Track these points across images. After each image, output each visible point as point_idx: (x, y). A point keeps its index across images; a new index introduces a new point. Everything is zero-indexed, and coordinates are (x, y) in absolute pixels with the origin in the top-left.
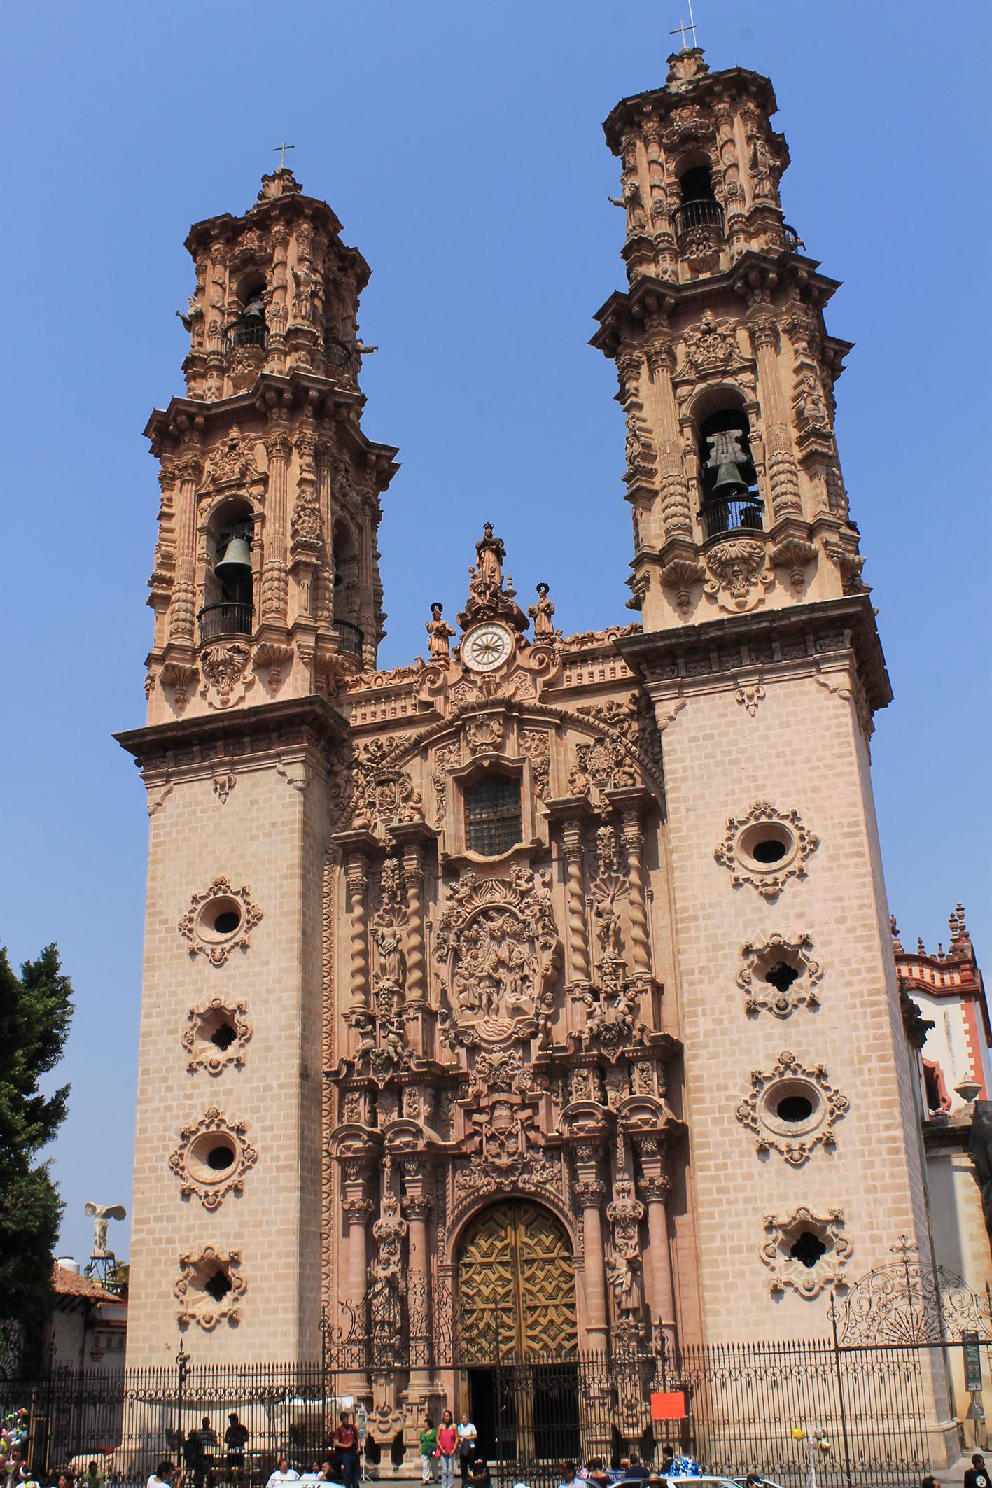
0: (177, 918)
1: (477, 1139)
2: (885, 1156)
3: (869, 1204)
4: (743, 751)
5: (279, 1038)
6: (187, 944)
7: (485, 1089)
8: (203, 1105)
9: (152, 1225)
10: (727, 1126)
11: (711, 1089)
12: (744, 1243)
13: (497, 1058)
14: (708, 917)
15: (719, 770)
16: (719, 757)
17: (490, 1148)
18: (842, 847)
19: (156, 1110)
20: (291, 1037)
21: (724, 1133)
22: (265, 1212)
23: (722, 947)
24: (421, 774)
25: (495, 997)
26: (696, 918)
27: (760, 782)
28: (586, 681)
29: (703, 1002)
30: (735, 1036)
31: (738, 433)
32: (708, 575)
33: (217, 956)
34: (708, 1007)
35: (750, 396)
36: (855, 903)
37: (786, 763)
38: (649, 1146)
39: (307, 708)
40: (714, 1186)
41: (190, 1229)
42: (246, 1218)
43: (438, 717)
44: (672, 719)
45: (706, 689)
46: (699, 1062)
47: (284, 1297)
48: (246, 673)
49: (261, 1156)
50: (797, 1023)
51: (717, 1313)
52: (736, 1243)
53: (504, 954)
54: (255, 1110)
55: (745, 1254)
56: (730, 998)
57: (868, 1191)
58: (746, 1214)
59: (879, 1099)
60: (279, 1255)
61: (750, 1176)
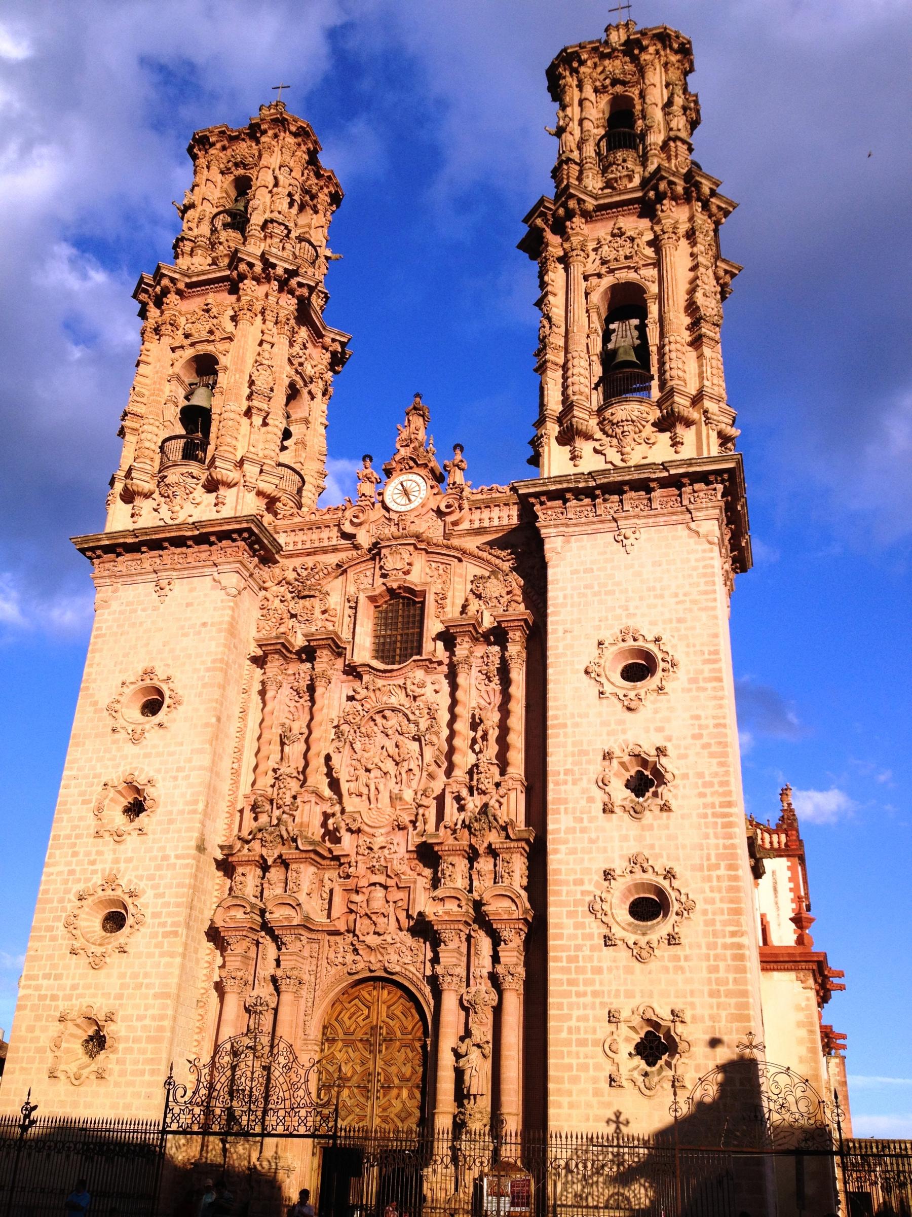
0: (104, 700)
1: (353, 916)
2: (730, 962)
3: (712, 1007)
4: (618, 584)
5: (182, 812)
6: (110, 722)
7: (362, 868)
8: (103, 870)
9: (40, 981)
10: (580, 919)
11: (567, 883)
12: (590, 1037)
13: (380, 841)
14: (576, 725)
15: (596, 599)
16: (596, 588)
17: (363, 925)
18: (702, 672)
19: (59, 873)
20: (195, 812)
21: (577, 926)
22: (146, 975)
23: (586, 753)
24: (336, 594)
25: (381, 787)
26: (565, 726)
27: (632, 611)
28: (486, 524)
29: (566, 801)
30: (593, 836)
31: (635, 322)
32: (598, 435)
33: (136, 736)
34: (570, 806)
35: (654, 289)
36: (711, 722)
37: (656, 597)
39: (245, 525)
40: (565, 977)
41: (74, 987)
42: (127, 980)
43: (356, 547)
44: (557, 553)
45: (589, 529)
46: (558, 856)
47: (152, 1059)
49: (148, 920)
50: (651, 827)
51: (560, 1106)
52: (582, 1036)
53: (393, 750)
54: (151, 878)
55: (590, 1048)
56: (591, 800)
57: (712, 994)
58: (593, 1007)
59: (726, 906)
60: (153, 1018)
61: (598, 970)
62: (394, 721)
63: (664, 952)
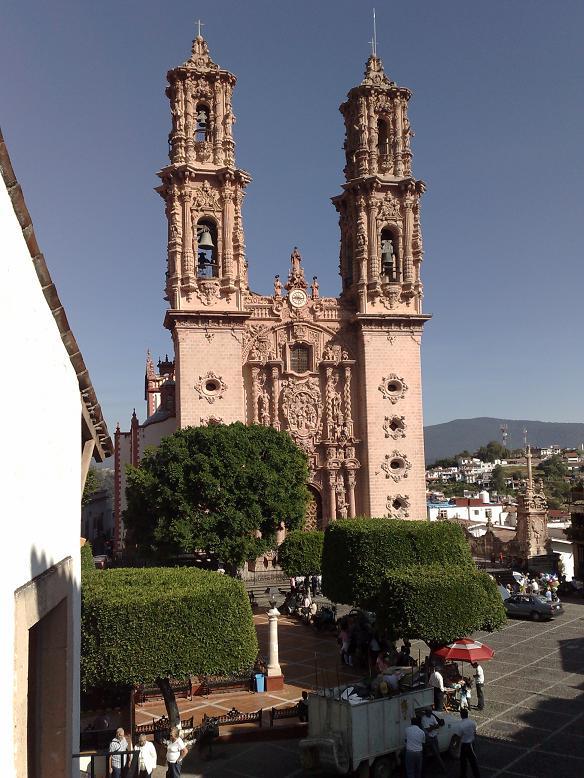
38: (353, 472)
62: (305, 398)
63: (403, 479)
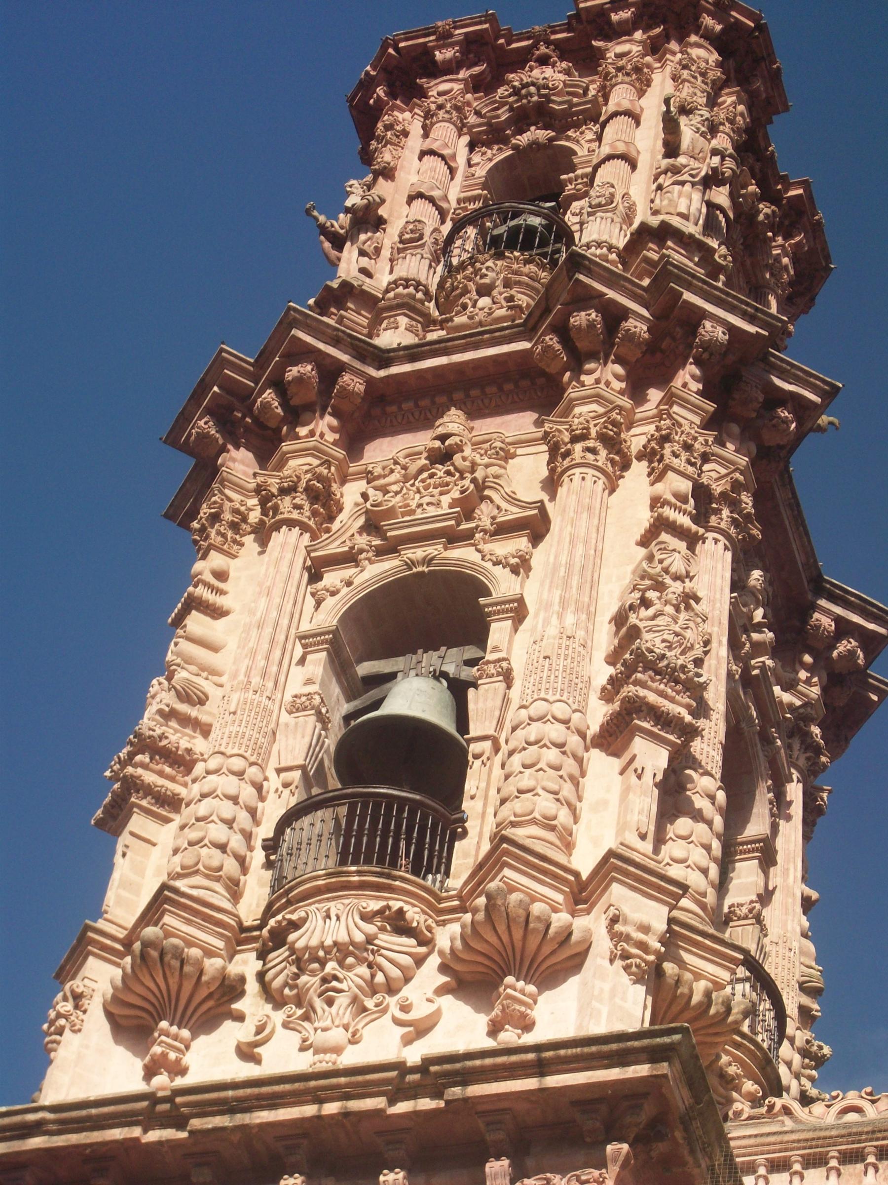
48: (407, 992)
